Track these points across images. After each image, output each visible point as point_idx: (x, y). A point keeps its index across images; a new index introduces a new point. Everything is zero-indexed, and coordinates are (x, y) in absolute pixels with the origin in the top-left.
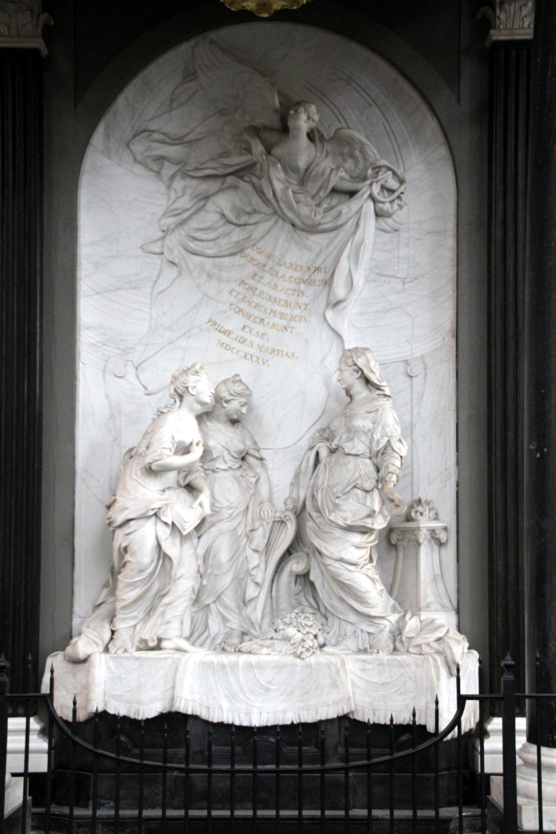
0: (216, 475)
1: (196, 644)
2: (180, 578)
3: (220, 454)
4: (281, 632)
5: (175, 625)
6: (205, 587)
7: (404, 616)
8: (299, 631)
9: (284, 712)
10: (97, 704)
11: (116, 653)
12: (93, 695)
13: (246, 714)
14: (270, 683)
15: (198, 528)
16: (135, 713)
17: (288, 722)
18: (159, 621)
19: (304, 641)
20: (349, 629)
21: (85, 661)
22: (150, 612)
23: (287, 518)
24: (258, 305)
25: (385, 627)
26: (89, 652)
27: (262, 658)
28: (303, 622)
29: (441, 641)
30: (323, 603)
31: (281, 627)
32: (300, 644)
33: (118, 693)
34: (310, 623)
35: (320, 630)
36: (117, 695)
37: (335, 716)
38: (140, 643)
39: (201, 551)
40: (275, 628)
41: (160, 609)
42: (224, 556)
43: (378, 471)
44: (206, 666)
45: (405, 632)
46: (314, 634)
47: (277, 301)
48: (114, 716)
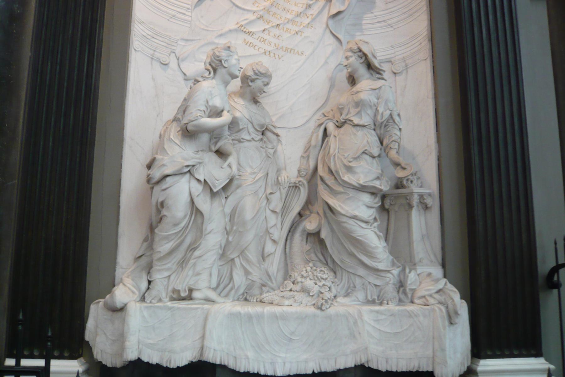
0: (242, 145)
1: (222, 295)
2: (210, 232)
3: (246, 126)
4: (300, 284)
5: (205, 276)
6: (231, 242)
7: (404, 270)
8: (316, 284)
9: (306, 361)
10: (131, 355)
11: (151, 302)
12: (127, 344)
13: (271, 363)
14: (293, 333)
15: (225, 188)
16: (167, 362)
17: (310, 372)
18: (190, 273)
19: (322, 293)
20: (358, 281)
21: (122, 309)
22: (183, 263)
23: (301, 183)
24: (275, 14)
25: (390, 281)
26: (125, 302)
27: (285, 309)
28: (319, 275)
29: (441, 293)
30: (331, 257)
31: (299, 279)
32: (319, 296)
33: (151, 341)
34: (325, 276)
35: (332, 282)
36: (150, 344)
37: (353, 366)
38: (173, 293)
39: (228, 210)
40: (292, 280)
41: (192, 262)
42: (248, 215)
43: (382, 143)
44: (233, 316)
45: (408, 285)
46: (329, 286)
47: (290, 11)
48: (148, 363)
